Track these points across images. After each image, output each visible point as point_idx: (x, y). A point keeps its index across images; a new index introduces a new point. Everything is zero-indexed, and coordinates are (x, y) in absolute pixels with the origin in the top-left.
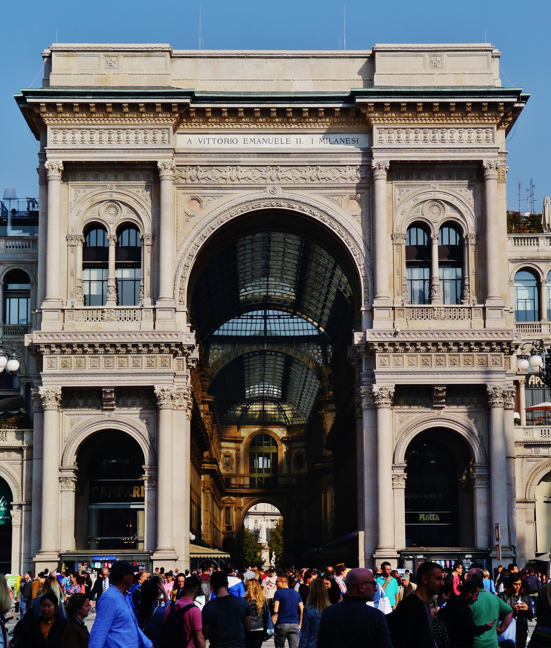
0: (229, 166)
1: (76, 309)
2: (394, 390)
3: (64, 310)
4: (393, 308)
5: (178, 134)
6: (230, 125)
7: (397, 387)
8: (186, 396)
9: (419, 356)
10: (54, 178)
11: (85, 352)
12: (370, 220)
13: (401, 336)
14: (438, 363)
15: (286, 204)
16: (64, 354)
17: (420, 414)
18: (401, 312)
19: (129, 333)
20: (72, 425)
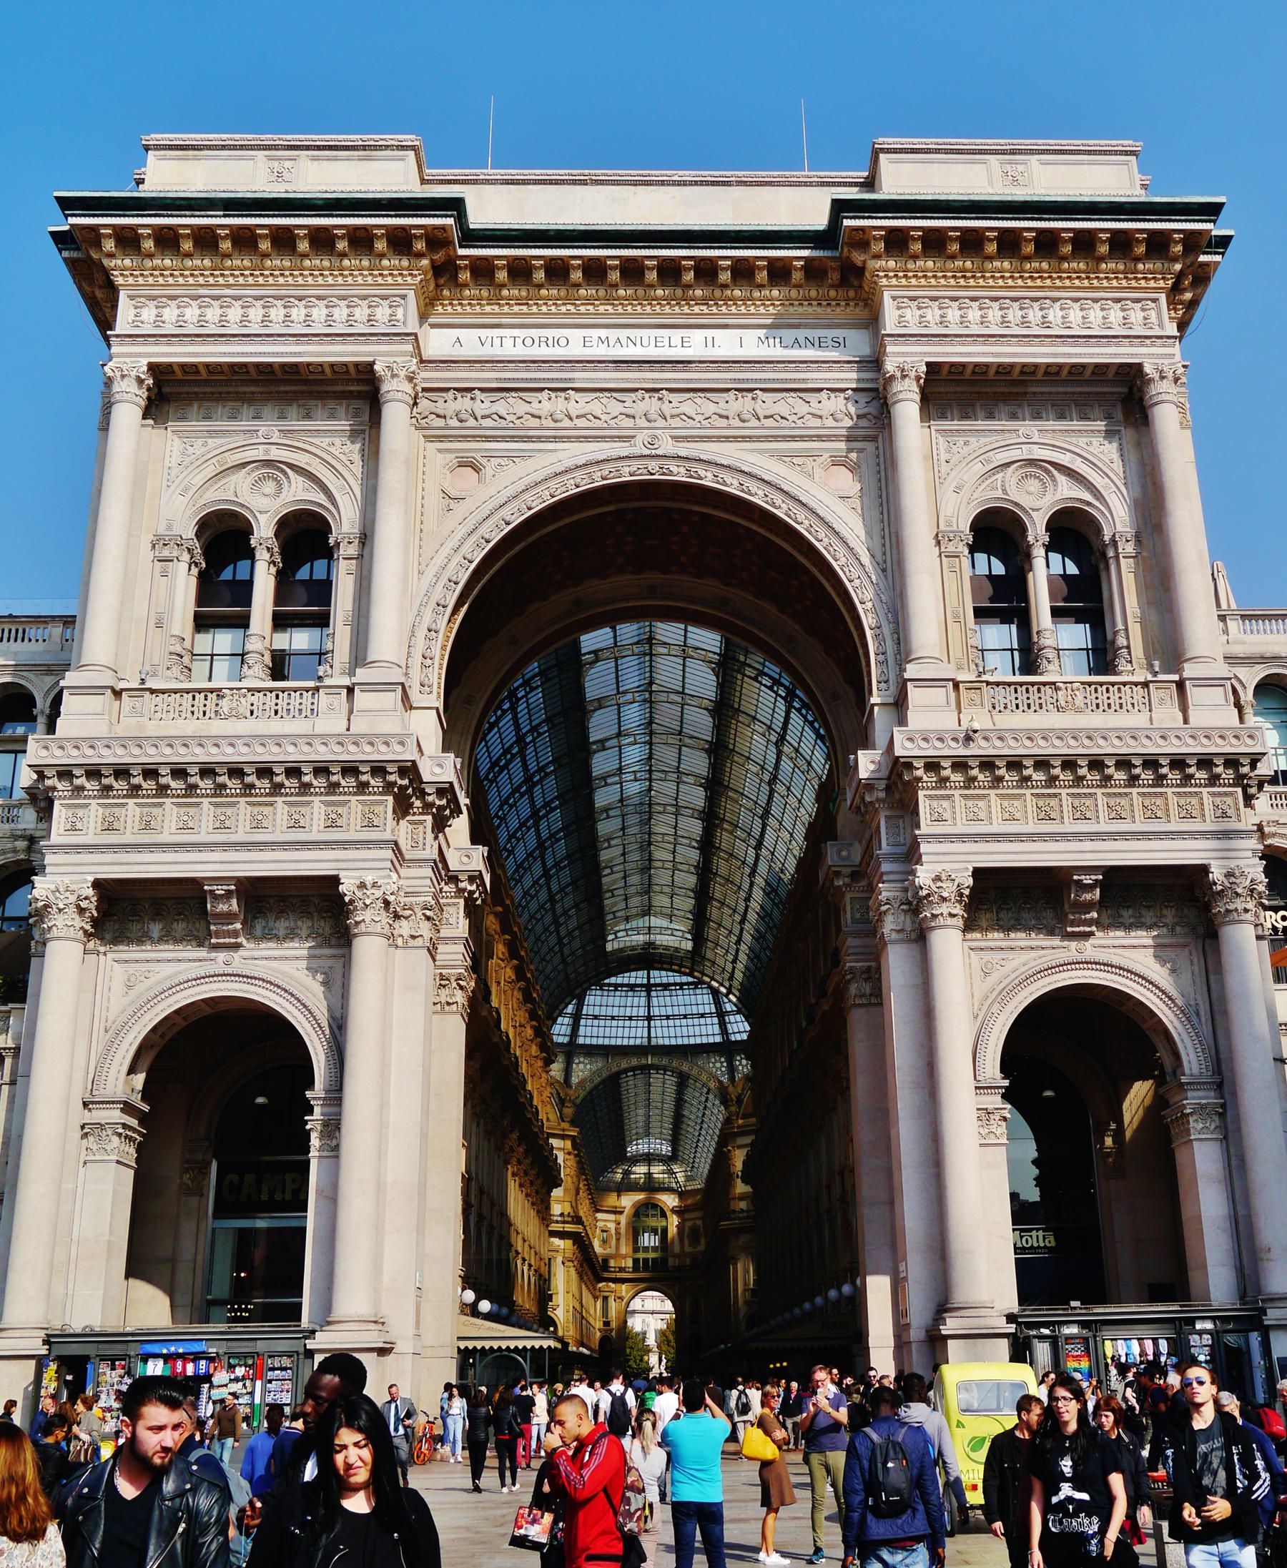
0: (549, 389)
1: (152, 691)
2: (970, 881)
3: (123, 690)
4: (956, 685)
5: (433, 326)
6: (551, 302)
7: (978, 873)
8: (428, 913)
9: (1029, 797)
10: (126, 396)
11: (163, 790)
12: (881, 505)
13: (983, 743)
14: (1078, 815)
15: (682, 470)
16: (108, 797)
17: (1033, 954)
18: (972, 694)
19: (279, 740)
20: (129, 987)
